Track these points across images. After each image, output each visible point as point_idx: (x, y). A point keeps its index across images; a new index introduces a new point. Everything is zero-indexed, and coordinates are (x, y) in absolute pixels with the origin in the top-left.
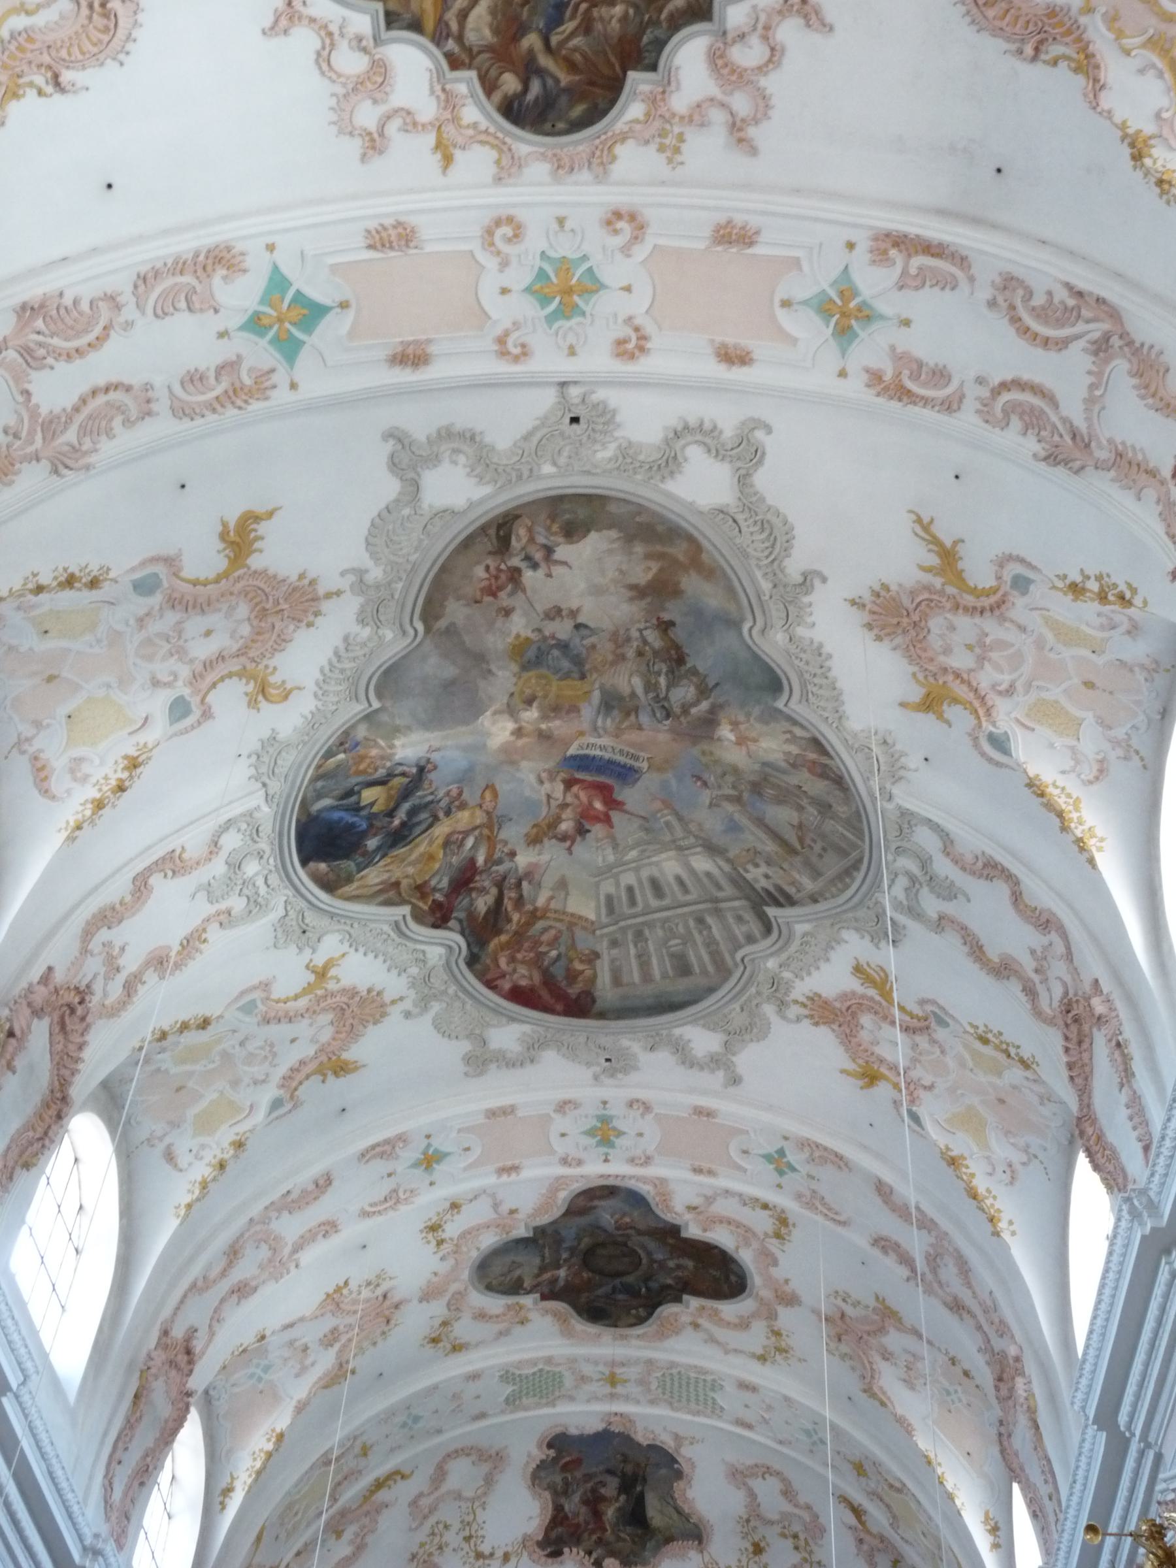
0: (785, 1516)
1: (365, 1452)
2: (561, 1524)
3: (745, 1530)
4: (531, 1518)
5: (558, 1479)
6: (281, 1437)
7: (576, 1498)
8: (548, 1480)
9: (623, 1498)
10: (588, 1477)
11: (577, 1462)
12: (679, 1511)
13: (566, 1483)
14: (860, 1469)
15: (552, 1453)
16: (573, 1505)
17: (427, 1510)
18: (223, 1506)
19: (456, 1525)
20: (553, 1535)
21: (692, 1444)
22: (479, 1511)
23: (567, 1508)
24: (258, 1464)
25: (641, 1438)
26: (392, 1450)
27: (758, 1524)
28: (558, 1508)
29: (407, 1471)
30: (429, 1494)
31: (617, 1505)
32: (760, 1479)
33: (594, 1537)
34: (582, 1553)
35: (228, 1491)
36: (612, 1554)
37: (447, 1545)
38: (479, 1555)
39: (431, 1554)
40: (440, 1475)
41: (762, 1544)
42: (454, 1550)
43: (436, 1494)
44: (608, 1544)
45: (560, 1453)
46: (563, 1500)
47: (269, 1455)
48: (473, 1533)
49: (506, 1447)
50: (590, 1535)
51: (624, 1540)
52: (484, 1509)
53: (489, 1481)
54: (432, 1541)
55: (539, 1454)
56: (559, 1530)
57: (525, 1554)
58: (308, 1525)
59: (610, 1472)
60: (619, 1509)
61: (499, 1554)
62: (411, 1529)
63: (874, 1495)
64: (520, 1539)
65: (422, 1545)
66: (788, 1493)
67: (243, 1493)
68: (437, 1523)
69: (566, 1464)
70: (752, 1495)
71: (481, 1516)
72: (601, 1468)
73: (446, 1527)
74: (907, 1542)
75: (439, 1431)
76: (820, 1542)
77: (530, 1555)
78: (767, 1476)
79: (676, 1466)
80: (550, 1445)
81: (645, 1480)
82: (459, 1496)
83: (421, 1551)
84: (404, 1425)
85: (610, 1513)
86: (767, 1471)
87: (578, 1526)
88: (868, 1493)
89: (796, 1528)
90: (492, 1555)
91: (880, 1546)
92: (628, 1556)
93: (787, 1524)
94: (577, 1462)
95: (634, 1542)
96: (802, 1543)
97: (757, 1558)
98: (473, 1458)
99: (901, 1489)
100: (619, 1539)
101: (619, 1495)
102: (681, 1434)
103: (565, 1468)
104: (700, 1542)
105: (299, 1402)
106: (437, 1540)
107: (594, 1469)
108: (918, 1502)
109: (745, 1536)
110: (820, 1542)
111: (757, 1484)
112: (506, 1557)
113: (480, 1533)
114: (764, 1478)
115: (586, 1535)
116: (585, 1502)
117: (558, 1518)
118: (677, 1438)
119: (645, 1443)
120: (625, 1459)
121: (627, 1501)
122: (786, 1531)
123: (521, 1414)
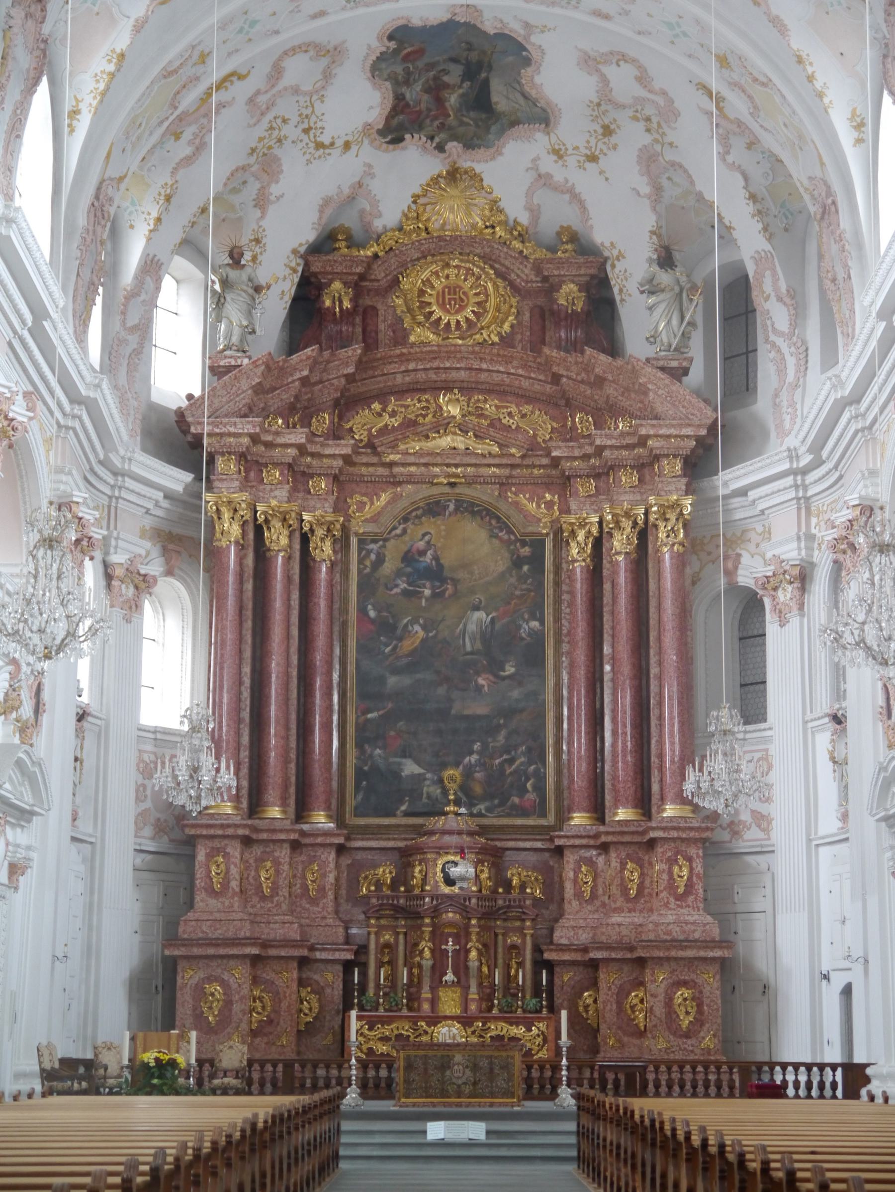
0: (638, 100)
1: (204, 58)
2: (402, 112)
3: (596, 113)
4: (371, 107)
5: (399, 69)
6: (122, 56)
7: (418, 87)
8: (389, 71)
9: (467, 84)
10: (431, 66)
11: (420, 52)
12: (525, 96)
13: (408, 72)
14: (723, 61)
15: (393, 45)
16: (414, 93)
17: (264, 106)
18: (72, 130)
19: (295, 119)
20: (395, 122)
21: (543, 32)
22: (317, 105)
23: (408, 96)
24: (102, 86)
25: (490, 27)
26: (230, 54)
27: (609, 107)
28: (399, 98)
29: (244, 72)
30: (266, 92)
31: (461, 91)
32: (614, 66)
33: (437, 123)
34: (424, 139)
35: (75, 113)
36: (455, 138)
37: (286, 138)
38: (319, 146)
39: (270, 148)
40: (277, 71)
41: (612, 127)
42: (293, 142)
43: (274, 91)
44: (450, 128)
45: (401, 44)
46: (403, 89)
47: (112, 75)
48: (312, 125)
49: (345, 42)
50: (432, 121)
51: (468, 124)
52: (322, 102)
53: (327, 76)
54: (270, 135)
55: (379, 47)
56: (401, 117)
57: (366, 142)
58: (151, 134)
59: (454, 60)
60: (462, 96)
61: (339, 143)
62: (249, 126)
63: (735, 85)
64: (360, 129)
65: (261, 139)
66: (643, 79)
67: (90, 116)
68: (275, 118)
69: (408, 54)
70: (605, 80)
71: (319, 108)
72: (445, 57)
73: (285, 121)
74: (766, 130)
75: (277, 32)
76: (673, 125)
77: (371, 143)
78: (622, 63)
79: (524, 53)
80: (390, 38)
81: (490, 67)
82: (296, 91)
83: (260, 145)
84: (241, 30)
85: (453, 99)
86: (623, 58)
87: (420, 113)
88: (730, 84)
89: (649, 111)
90: (332, 144)
91: (737, 130)
92: (472, 139)
93: (639, 108)
94: (420, 52)
95: (477, 126)
96: (655, 125)
97: (606, 140)
98: (312, 53)
99: (766, 84)
100: (462, 123)
101: (462, 82)
102: (532, 22)
103: (406, 59)
104: (547, 125)
105: (137, 20)
106: (276, 133)
107: (437, 58)
108: (784, 97)
109: (595, 119)
110: (673, 125)
111: (611, 71)
112: (347, 146)
113: (319, 124)
114: (619, 65)
115: (428, 121)
116: (427, 90)
117: (399, 106)
118: (527, 25)
119: (492, 32)
120: (470, 47)
121: (471, 87)
122: (639, 115)
123: (361, 11)
